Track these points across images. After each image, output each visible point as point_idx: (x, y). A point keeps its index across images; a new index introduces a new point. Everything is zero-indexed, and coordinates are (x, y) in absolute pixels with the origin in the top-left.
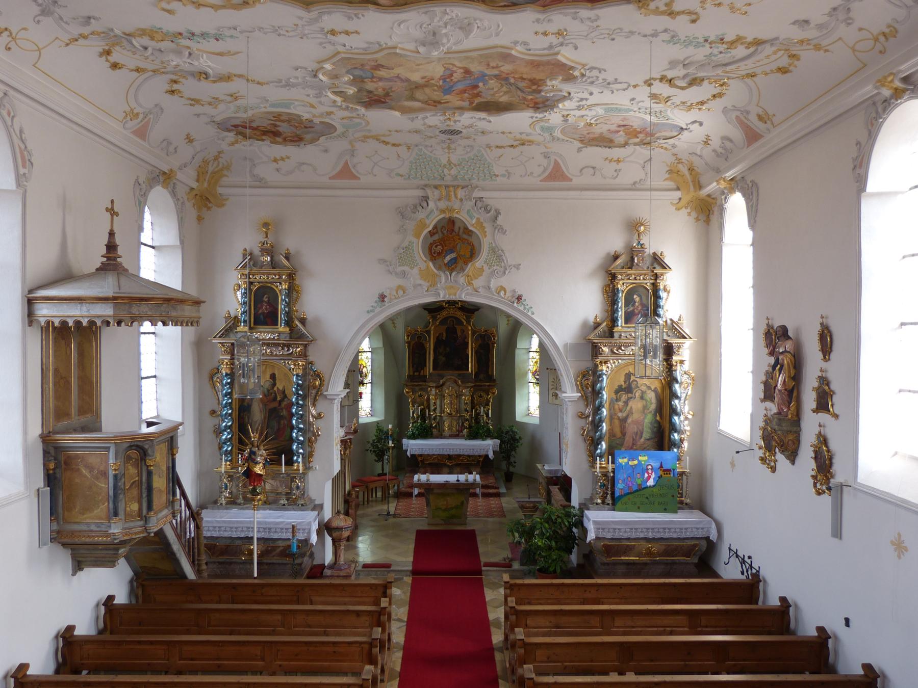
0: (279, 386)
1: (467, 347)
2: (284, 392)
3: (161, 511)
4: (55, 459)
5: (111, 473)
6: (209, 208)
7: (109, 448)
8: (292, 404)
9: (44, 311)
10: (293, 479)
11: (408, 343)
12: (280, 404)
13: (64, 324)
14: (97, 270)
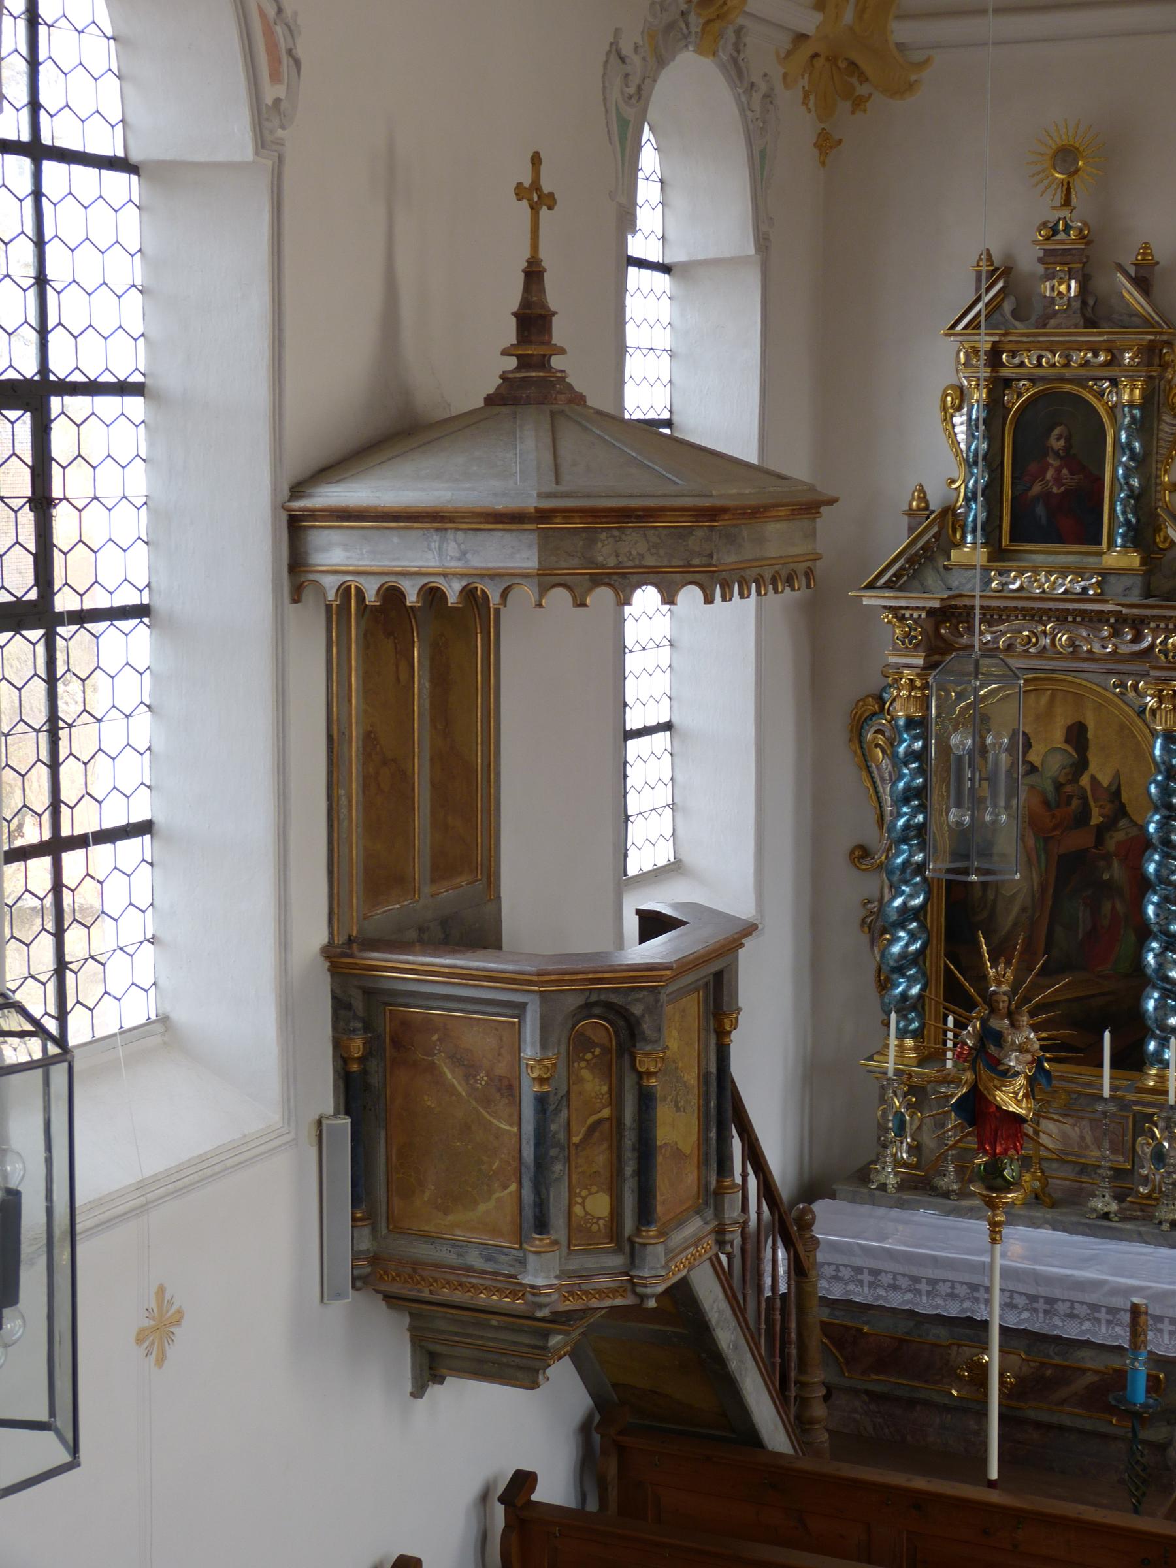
0: (1100, 770)
3: (680, 1222)
4: (368, 1027)
5: (529, 1090)
6: (859, 103)
7: (522, 1006)
8: (1145, 844)
9: (336, 554)
12: (1100, 840)
13: (392, 595)
14: (490, 400)
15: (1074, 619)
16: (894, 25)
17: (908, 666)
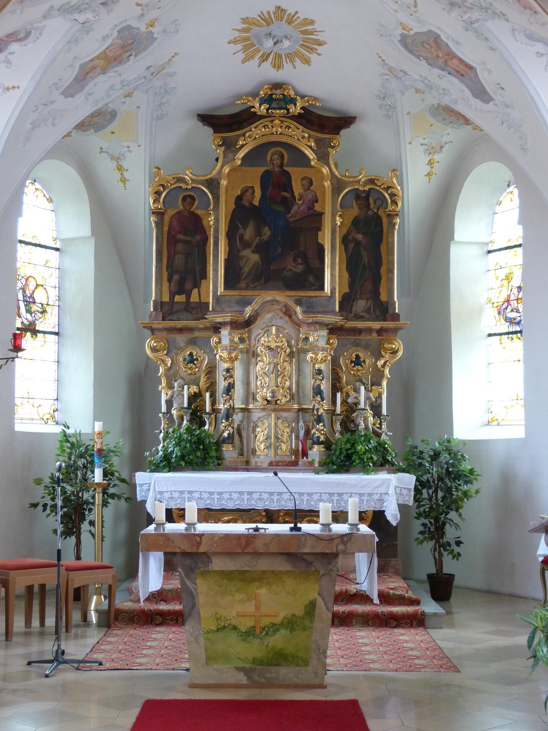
1: (319, 228)
11: (159, 214)
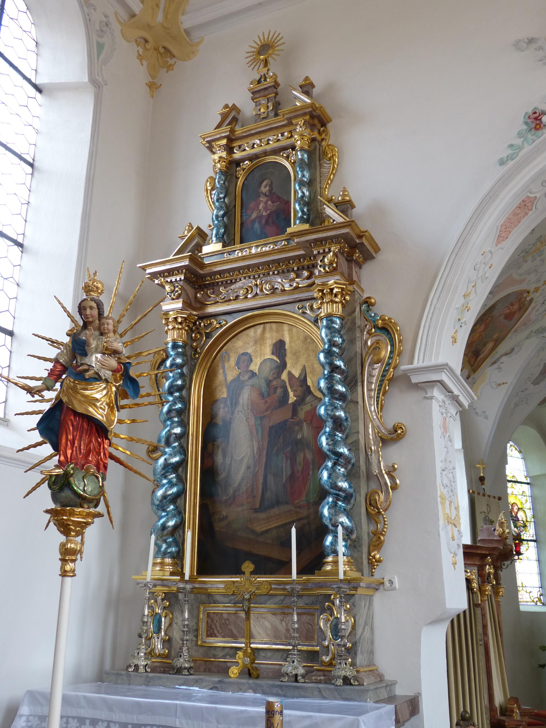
2: (303, 380)
6: (169, 67)
10: (323, 604)
12: (295, 412)
15: (274, 273)
16: (182, 18)
17: (173, 310)
